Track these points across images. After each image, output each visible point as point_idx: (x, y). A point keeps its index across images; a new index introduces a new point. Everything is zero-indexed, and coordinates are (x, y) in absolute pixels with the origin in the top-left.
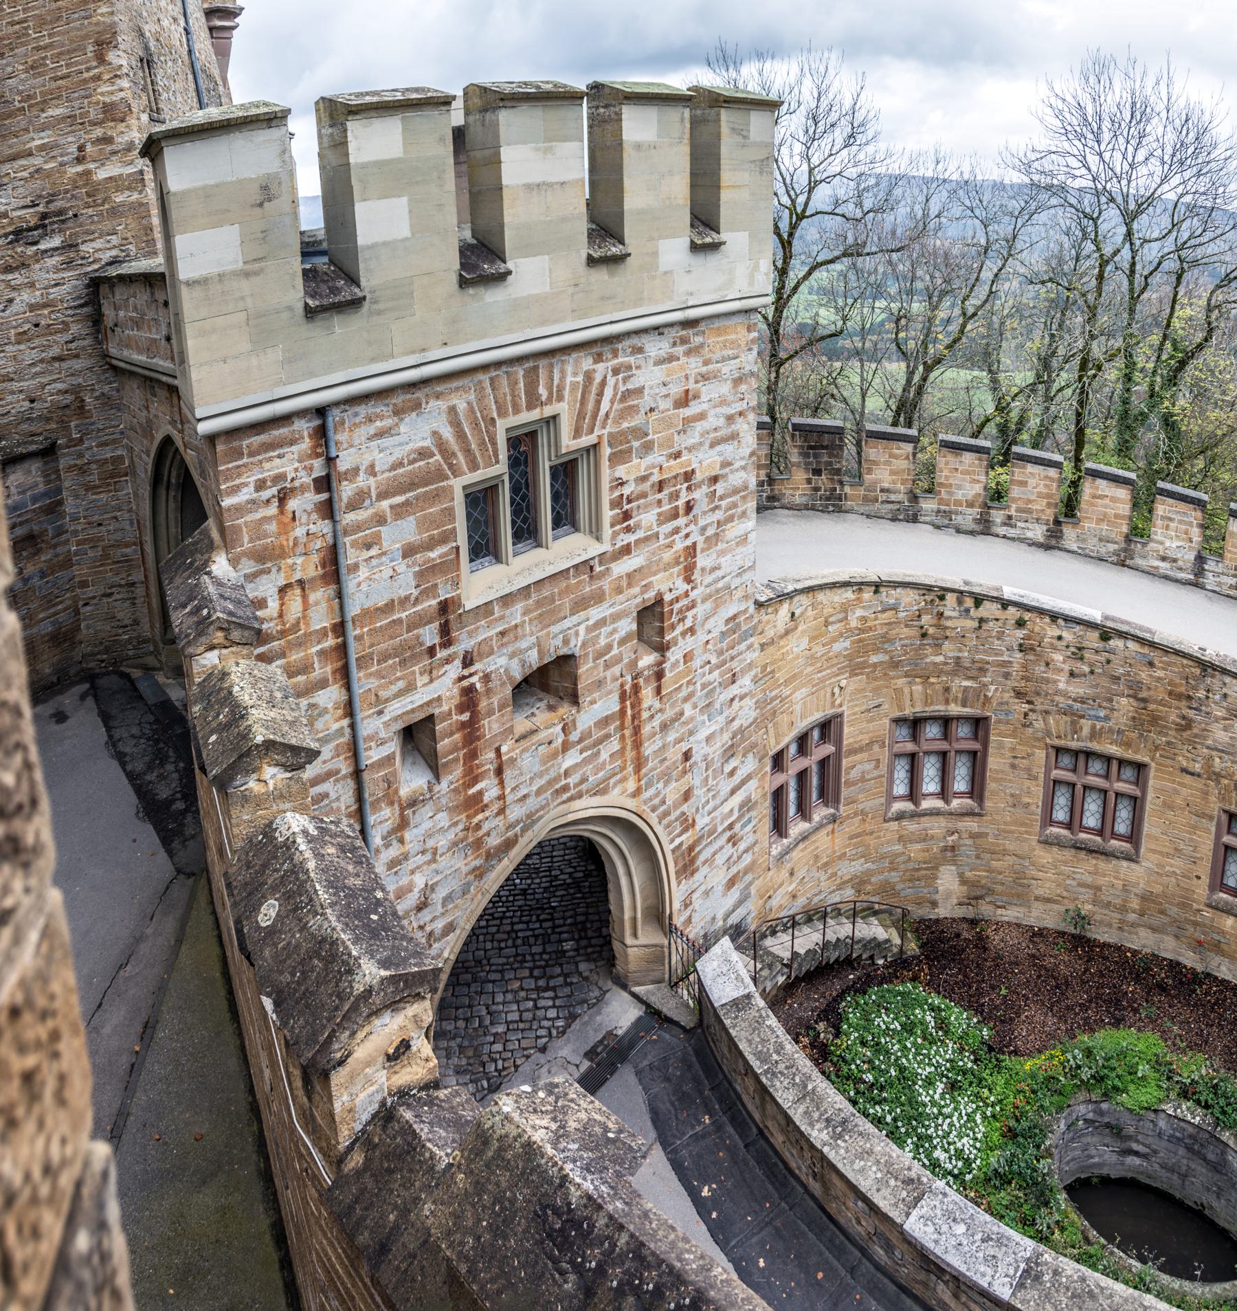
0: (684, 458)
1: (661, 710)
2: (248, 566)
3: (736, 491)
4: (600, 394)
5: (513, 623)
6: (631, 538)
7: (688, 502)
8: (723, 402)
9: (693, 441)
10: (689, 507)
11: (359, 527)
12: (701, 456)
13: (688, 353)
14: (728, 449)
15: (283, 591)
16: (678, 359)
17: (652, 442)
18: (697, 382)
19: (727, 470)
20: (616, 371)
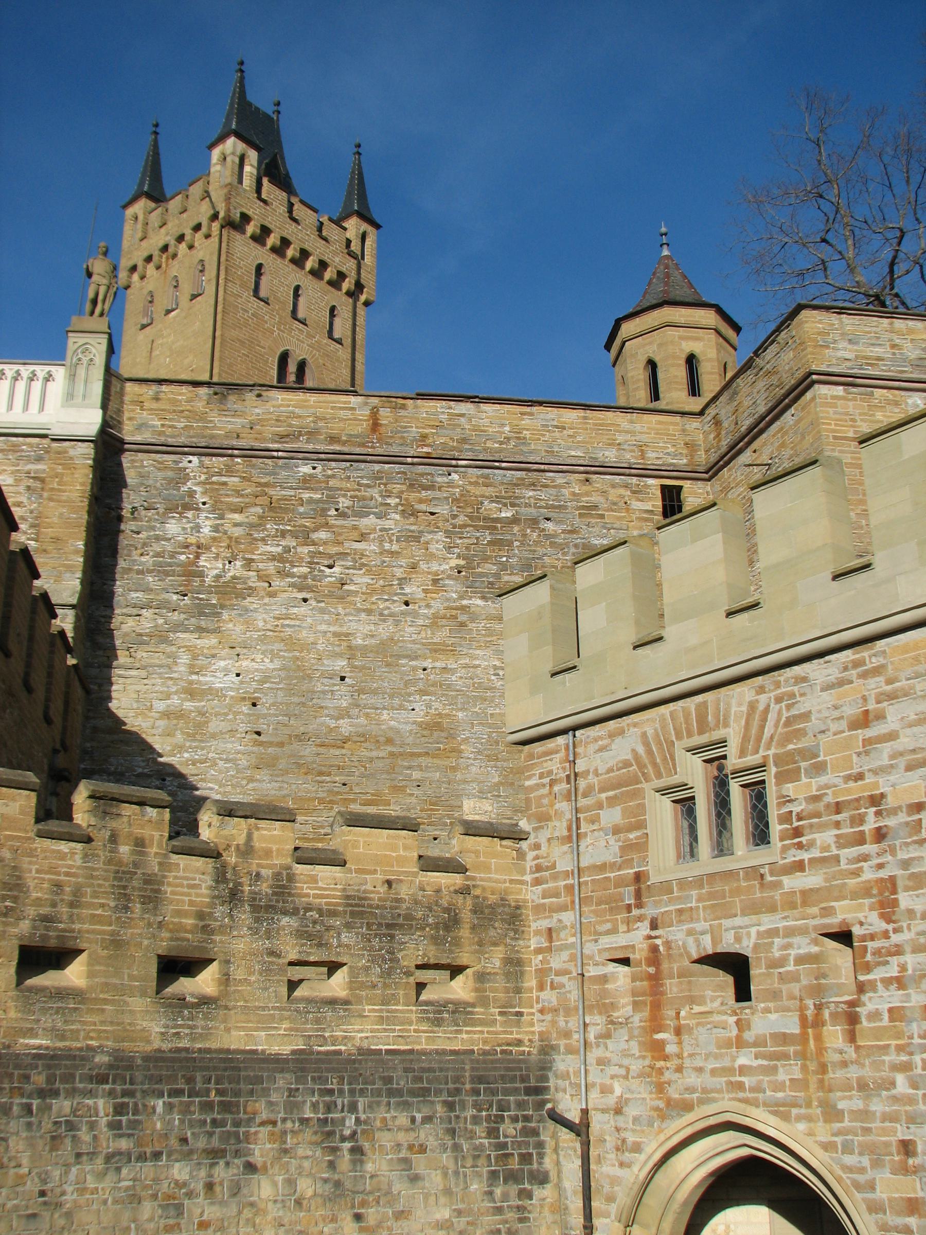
0: (867, 781)
1: (857, 1062)
4: (764, 720)
5: (689, 905)
6: (805, 856)
7: (879, 829)
9: (880, 763)
10: (880, 835)
11: (588, 809)
12: (892, 778)
13: (864, 675)
15: (549, 840)
16: (851, 682)
17: (824, 763)
20: (779, 700)
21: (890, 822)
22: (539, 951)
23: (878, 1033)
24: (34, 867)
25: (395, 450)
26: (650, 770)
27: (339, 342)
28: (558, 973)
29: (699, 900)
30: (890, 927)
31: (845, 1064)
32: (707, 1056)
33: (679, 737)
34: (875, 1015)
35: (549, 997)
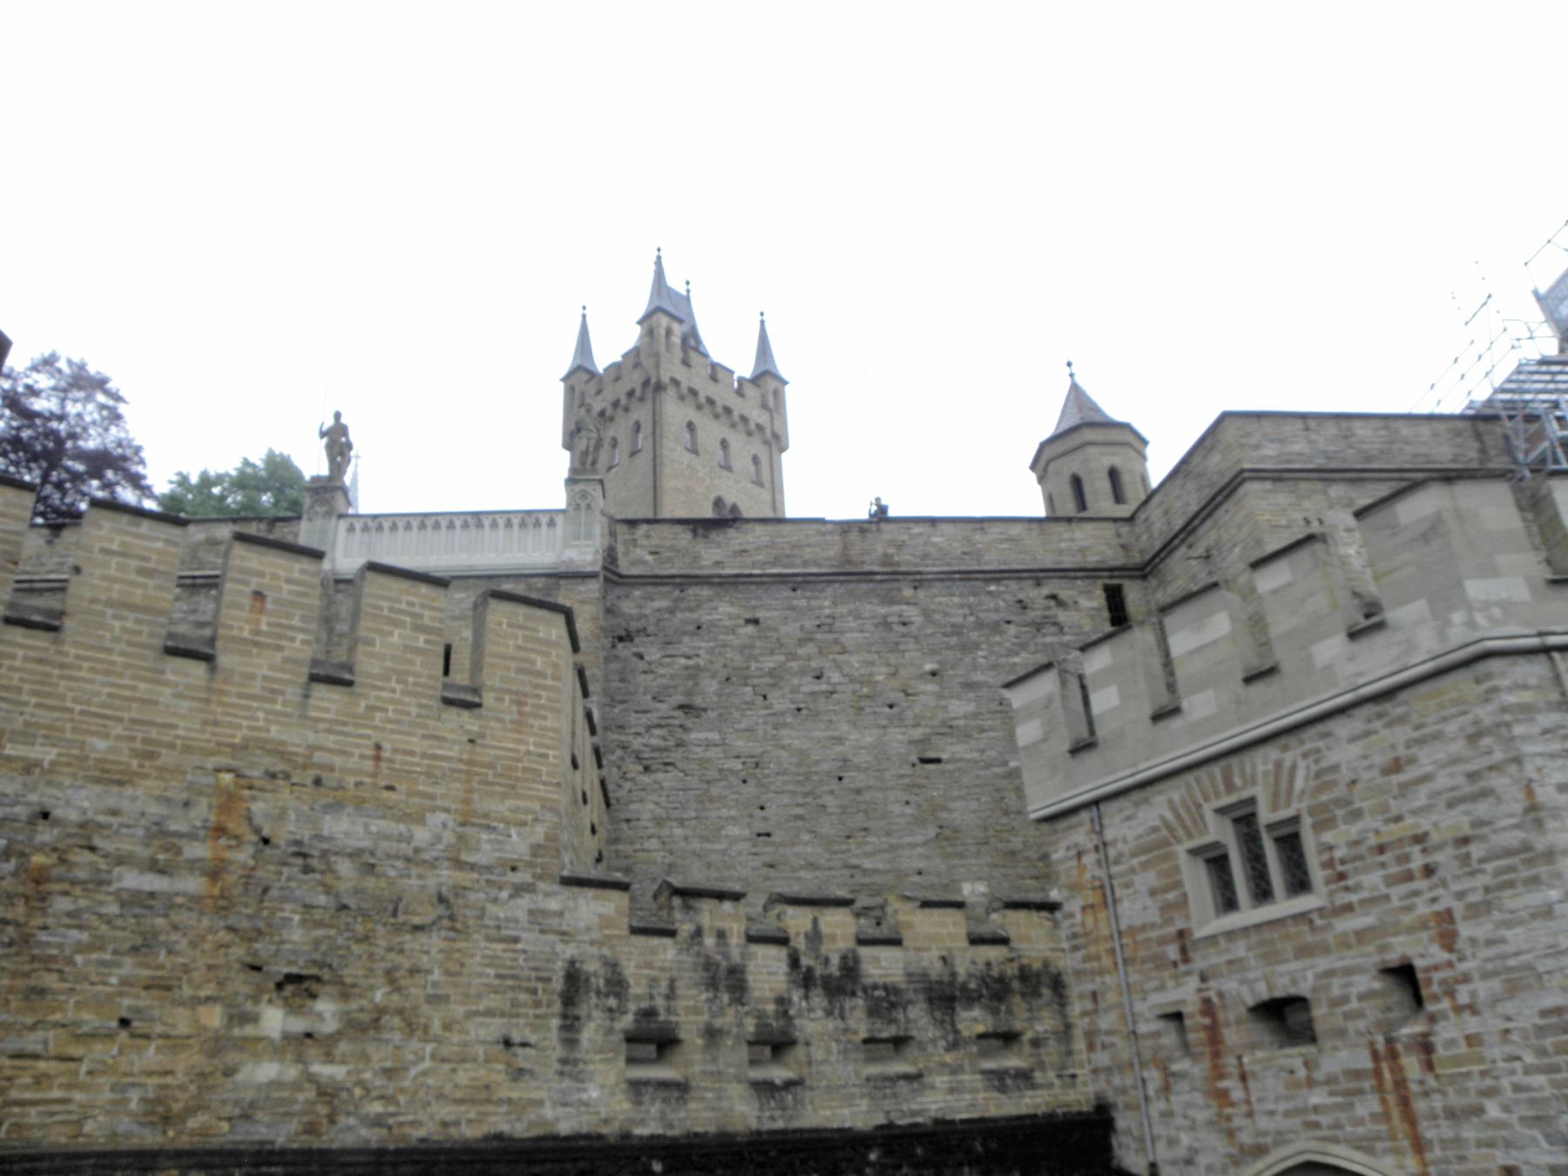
2: (1066, 893)
3: (1508, 853)
6: (1354, 898)
8: (1455, 760)
10: (1429, 871)
11: (1120, 875)
12: (1435, 818)
13: (1390, 724)
14: (1482, 809)
16: (1375, 732)
18: (1408, 747)
19: (1485, 830)
21: (1439, 857)
22: (1085, 1014)
23: (1458, 1060)
24: (632, 964)
25: (866, 568)
26: (1180, 832)
27: (760, 484)
28: (1109, 1033)
29: (1249, 949)
30: (1453, 957)
31: (1426, 1094)
32: (1278, 1099)
33: (1207, 799)
34: (1451, 1043)
35: (1102, 1058)
